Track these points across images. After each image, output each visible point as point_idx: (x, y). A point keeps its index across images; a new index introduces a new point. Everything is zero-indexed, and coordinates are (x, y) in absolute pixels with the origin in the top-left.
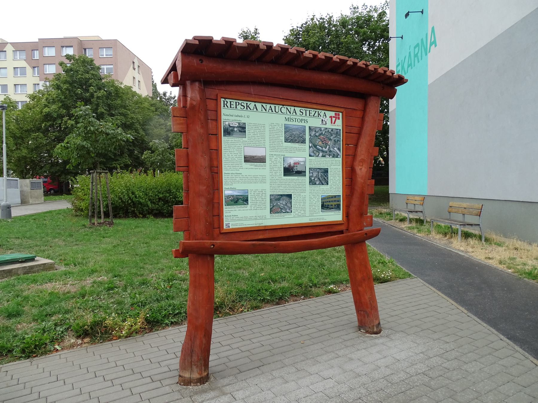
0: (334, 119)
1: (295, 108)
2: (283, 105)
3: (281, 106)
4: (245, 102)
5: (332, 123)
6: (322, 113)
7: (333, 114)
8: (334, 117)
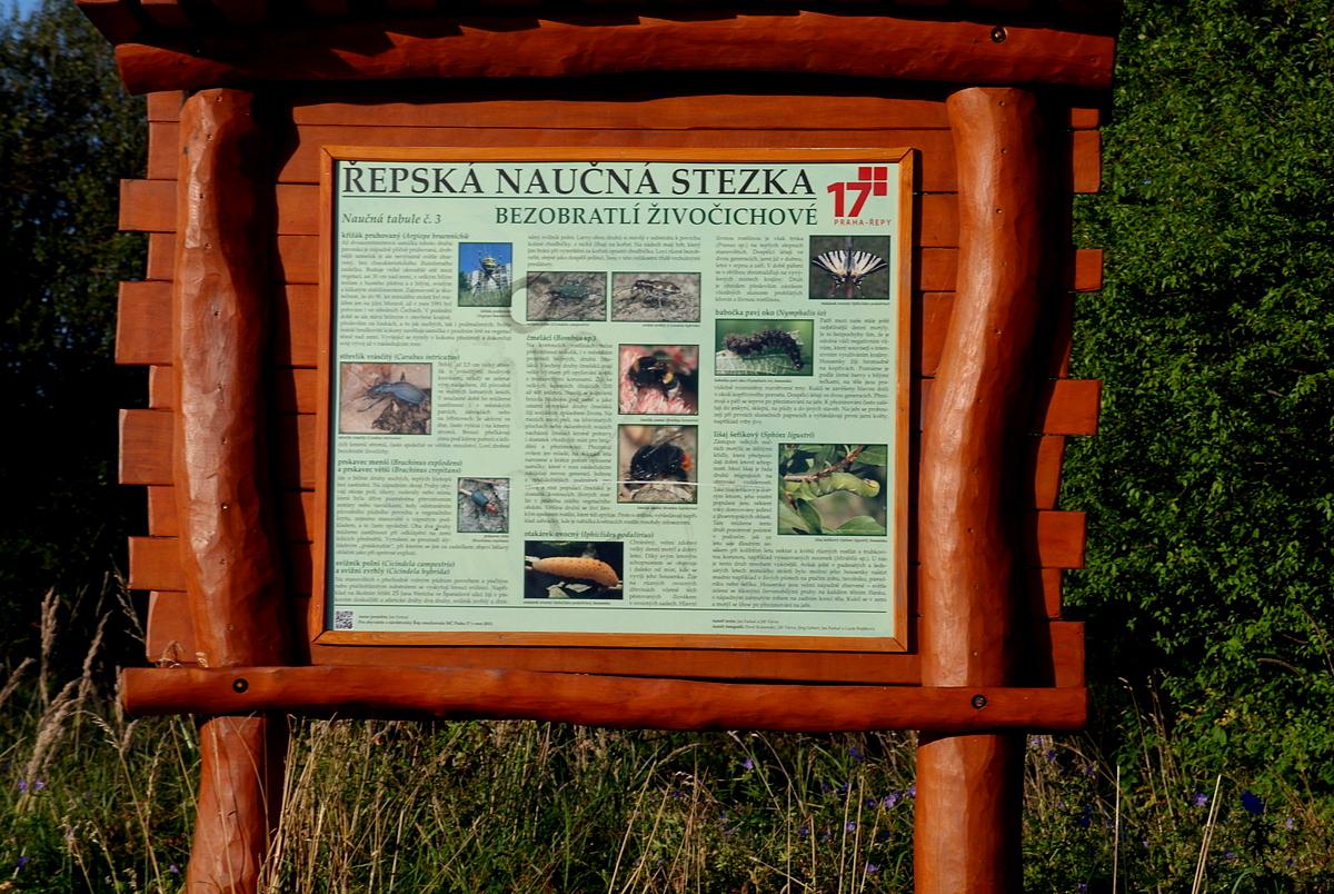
0: (851, 197)
2: (594, 162)
3: (583, 167)
4: (430, 166)
5: (839, 212)
6: (788, 176)
7: (849, 173)
8: (852, 186)
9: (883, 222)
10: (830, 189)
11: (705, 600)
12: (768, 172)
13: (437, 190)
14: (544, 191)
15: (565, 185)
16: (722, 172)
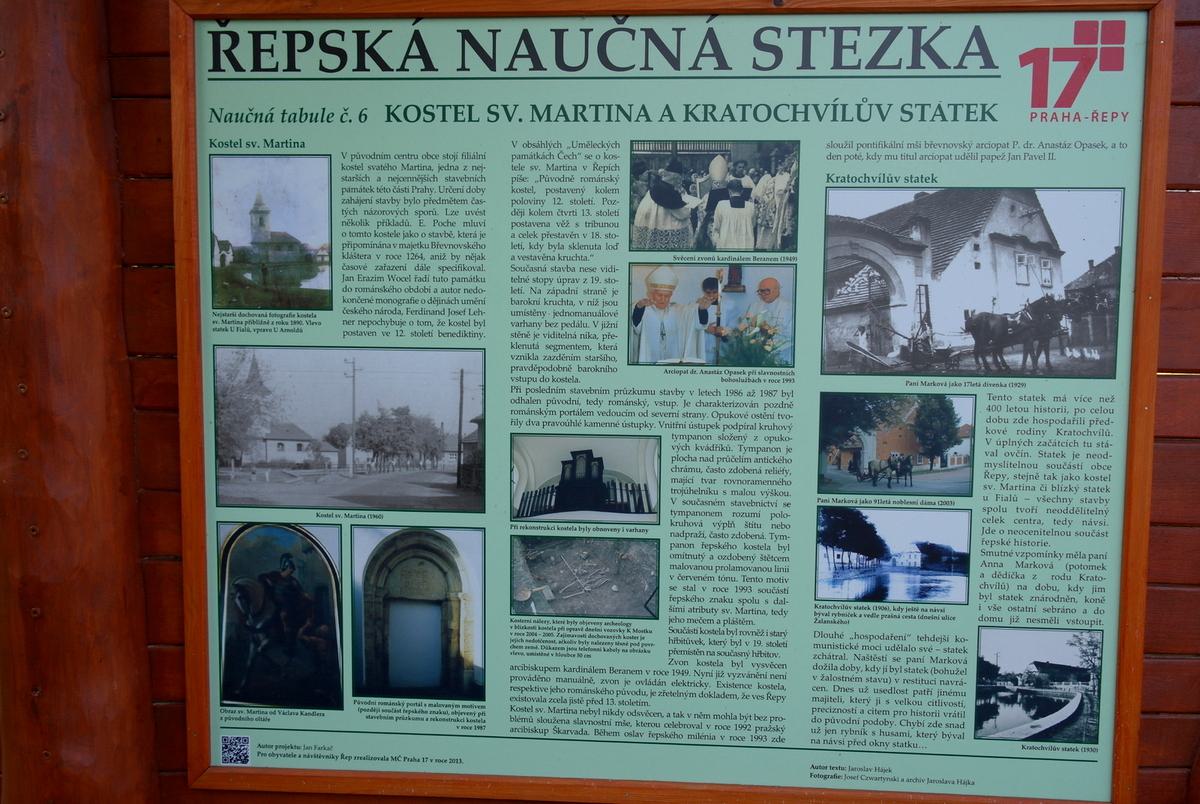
0: (1060, 74)
1: (721, 25)
2: (620, 15)
4: (349, 27)
5: (1039, 98)
7: (1057, 31)
8: (1062, 55)
9: (1114, 115)
10: (1025, 59)
11: (798, 731)
12: (917, 31)
13: (361, 67)
15: (572, 57)
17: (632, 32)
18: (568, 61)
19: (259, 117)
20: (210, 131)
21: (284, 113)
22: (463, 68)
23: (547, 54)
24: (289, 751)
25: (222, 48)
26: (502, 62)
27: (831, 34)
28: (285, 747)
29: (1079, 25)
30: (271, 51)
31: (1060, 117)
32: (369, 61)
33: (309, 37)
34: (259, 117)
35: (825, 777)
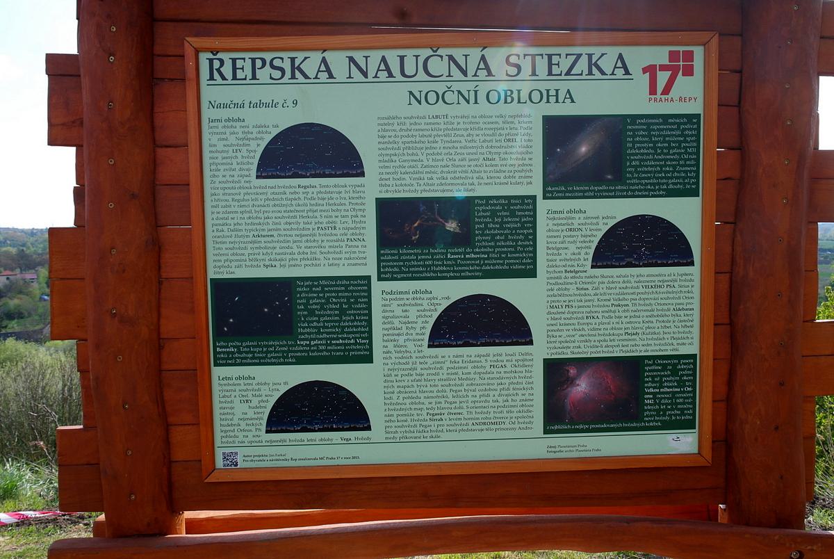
0: (662, 78)
3: (425, 53)
5: (653, 90)
7: (659, 55)
10: (645, 70)
12: (590, 56)
13: (293, 77)
14: (391, 75)
15: (409, 70)
16: (550, 56)
17: (441, 57)
18: (407, 73)
19: (236, 105)
20: (207, 113)
21: (250, 103)
22: (350, 77)
23: (395, 69)
24: (261, 458)
25: (215, 68)
26: (371, 74)
27: (546, 58)
28: (259, 456)
29: (671, 53)
30: (242, 69)
31: (663, 100)
32: (297, 74)
33: (264, 61)
34: (236, 105)
35: (555, 452)
